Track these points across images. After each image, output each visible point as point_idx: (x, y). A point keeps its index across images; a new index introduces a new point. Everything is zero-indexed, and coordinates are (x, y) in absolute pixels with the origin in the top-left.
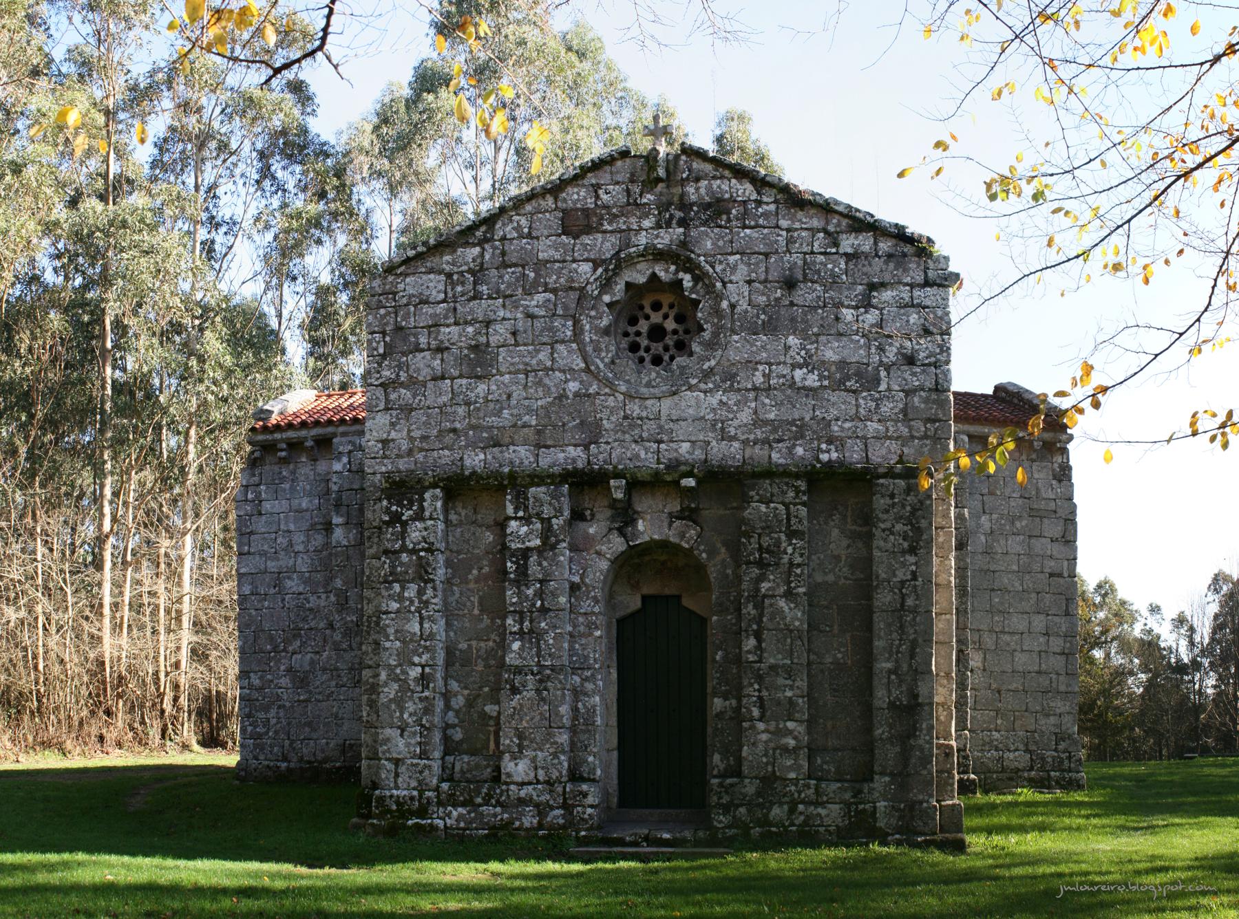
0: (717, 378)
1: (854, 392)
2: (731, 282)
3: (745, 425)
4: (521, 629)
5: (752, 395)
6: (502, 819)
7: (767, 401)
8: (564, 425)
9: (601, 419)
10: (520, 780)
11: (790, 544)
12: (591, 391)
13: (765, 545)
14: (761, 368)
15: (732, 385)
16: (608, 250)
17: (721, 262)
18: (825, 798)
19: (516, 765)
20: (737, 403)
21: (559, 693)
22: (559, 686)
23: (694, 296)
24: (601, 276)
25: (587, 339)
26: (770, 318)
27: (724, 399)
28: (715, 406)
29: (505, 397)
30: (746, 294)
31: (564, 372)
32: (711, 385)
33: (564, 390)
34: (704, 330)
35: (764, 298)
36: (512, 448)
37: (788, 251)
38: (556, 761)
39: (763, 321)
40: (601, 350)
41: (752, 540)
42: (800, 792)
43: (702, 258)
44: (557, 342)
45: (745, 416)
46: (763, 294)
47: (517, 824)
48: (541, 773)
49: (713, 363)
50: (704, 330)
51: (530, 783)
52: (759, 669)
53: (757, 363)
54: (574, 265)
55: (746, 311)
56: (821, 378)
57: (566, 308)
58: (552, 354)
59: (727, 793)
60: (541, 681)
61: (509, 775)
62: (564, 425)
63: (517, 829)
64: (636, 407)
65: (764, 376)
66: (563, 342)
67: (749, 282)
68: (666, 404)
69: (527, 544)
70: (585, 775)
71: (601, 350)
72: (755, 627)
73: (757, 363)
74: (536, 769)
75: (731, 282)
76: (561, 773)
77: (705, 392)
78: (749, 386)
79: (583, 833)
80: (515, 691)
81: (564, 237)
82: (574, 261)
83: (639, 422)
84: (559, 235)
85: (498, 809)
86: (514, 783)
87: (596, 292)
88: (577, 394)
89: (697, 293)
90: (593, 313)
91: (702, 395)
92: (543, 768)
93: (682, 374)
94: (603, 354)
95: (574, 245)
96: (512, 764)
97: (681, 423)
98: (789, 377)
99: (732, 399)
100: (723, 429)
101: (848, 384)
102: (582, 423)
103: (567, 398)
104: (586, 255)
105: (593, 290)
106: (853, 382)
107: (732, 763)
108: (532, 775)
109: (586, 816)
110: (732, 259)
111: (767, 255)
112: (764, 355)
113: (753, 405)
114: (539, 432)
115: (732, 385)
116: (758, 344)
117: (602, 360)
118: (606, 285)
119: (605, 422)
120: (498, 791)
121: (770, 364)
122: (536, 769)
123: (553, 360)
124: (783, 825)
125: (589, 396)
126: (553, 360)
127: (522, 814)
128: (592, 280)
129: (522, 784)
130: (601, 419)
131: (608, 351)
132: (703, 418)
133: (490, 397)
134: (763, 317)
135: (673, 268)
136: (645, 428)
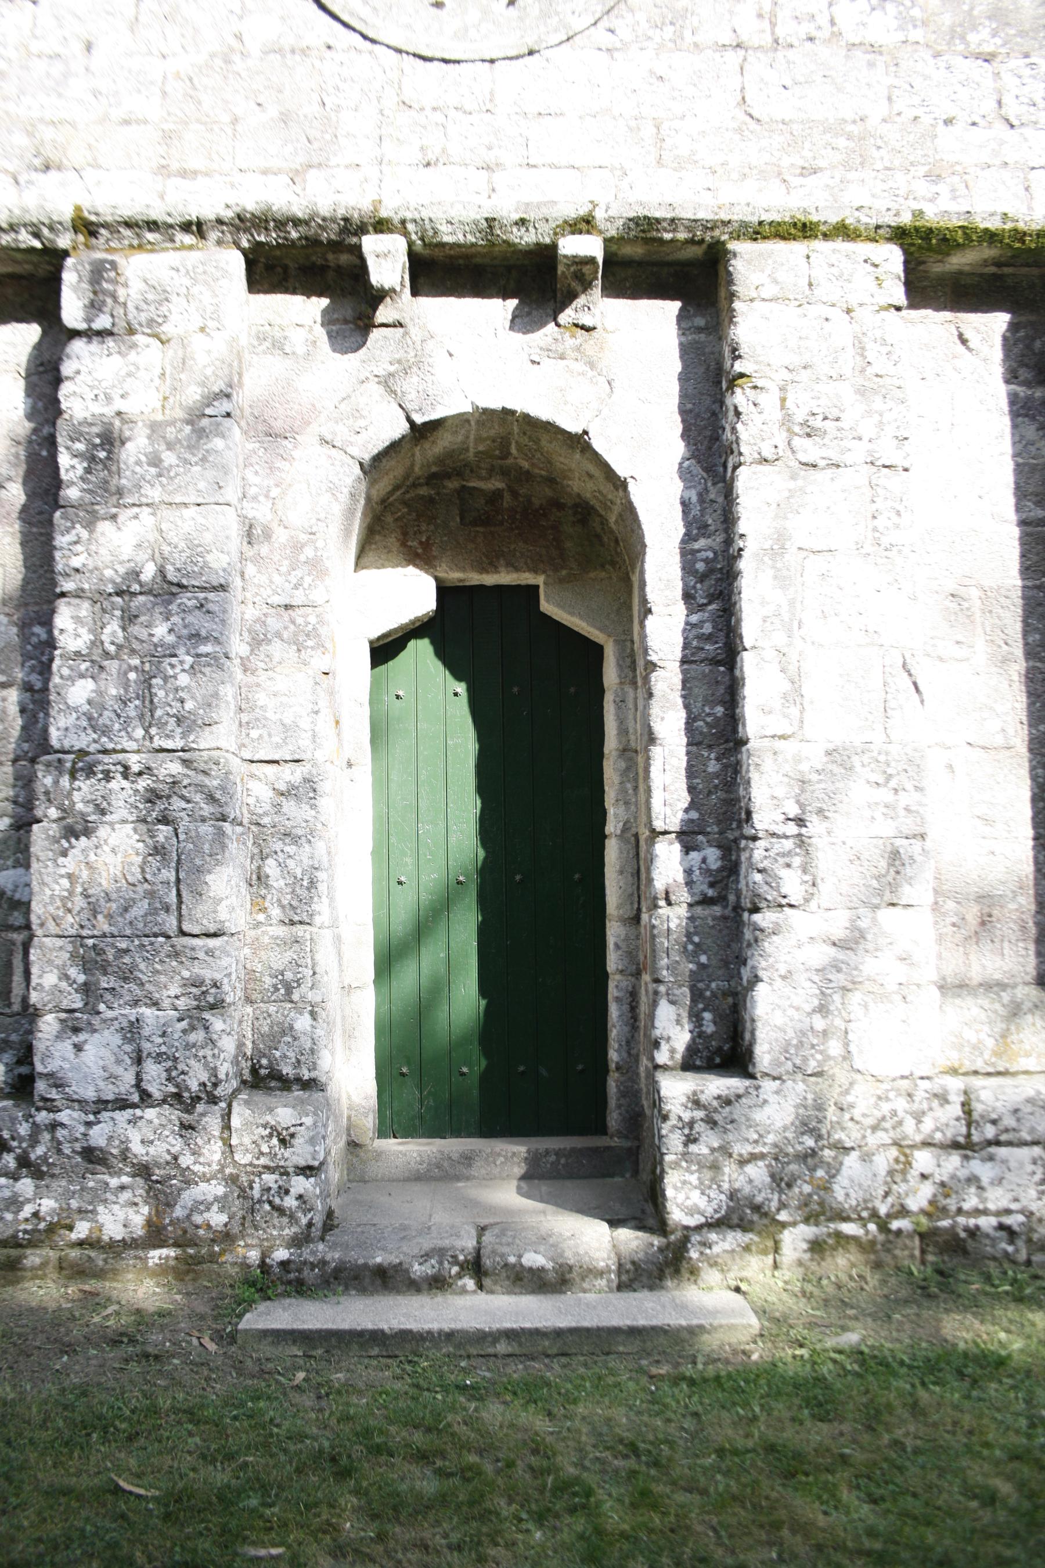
1: (988, 59)
4: (97, 642)
5: (734, 58)
6: (35, 1214)
8: (235, 121)
9: (338, 108)
10: (90, 1094)
11: (869, 413)
13: (800, 416)
18: (990, 1132)
19: (78, 1048)
21: (206, 829)
22: (207, 810)
29: (78, 47)
33: (239, 37)
36: (89, 173)
38: (198, 1036)
41: (761, 398)
42: (918, 1117)
47: (82, 1229)
48: (154, 1073)
51: (122, 1104)
52: (797, 760)
56: (906, 21)
59: (712, 1123)
60: (153, 797)
61: (57, 1082)
62: (235, 121)
63: (81, 1244)
69: (119, 405)
70: (287, 1070)
72: (780, 638)
74: (139, 1061)
76: (214, 1072)
79: (281, 1254)
80: (76, 829)
83: (438, 117)
85: (26, 1186)
86: (74, 1102)
92: (159, 1057)
96: (66, 1047)
98: (823, 20)
101: (973, 38)
102: (285, 119)
106: (985, 33)
107: (709, 1028)
108: (129, 1078)
109: (290, 1202)
114: (167, 137)
120: (24, 1129)
122: (139, 1061)
124: (874, 1215)
125: (305, 51)
127: (100, 1196)
129: (101, 1105)
130: (338, 108)
133: (35, 47)
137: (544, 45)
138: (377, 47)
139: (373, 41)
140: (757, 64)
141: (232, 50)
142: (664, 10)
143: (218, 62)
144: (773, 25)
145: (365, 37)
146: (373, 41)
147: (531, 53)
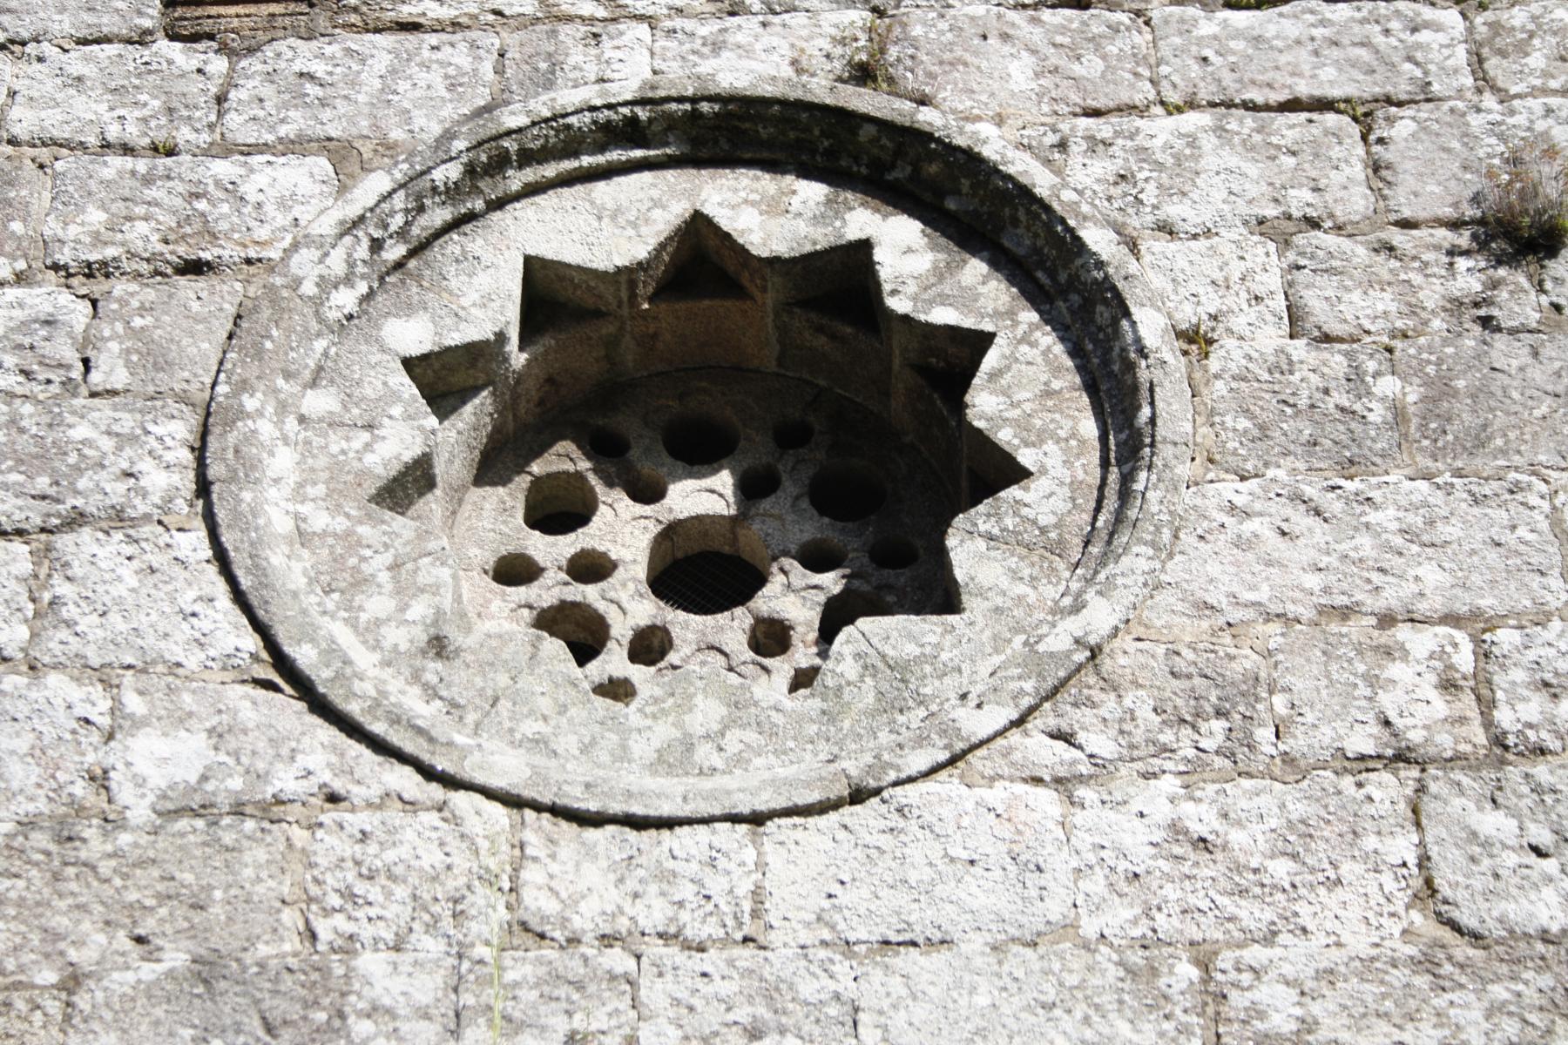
0: (1141, 702)
2: (1167, 229)
3: (1367, 966)
5: (1387, 789)
7: (1493, 823)
8: (73, 981)
9: (349, 946)
12: (285, 781)
14: (1420, 642)
15: (1238, 750)
16: (430, 102)
17: (1096, 145)
20: (1294, 840)
23: (942, 316)
24: (376, 212)
25: (281, 523)
26: (1440, 391)
27: (1200, 817)
28: (1142, 858)
30: (1272, 281)
31: (105, 677)
32: (1100, 743)
33: (100, 779)
34: (1019, 474)
35: (1385, 302)
37: (1484, 82)
39: (1398, 413)
40: (361, 582)
43: (986, 129)
44: (76, 520)
45: (1360, 913)
46: (1371, 283)
49: (1099, 617)
50: (1019, 474)
53: (1387, 620)
54: (223, 168)
55: (1283, 366)
57: (152, 356)
58: (34, 584)
62: (73, 981)
64: (594, 875)
65: (1448, 685)
66: (119, 518)
67: (1280, 230)
68: (801, 859)
71: (361, 582)
73: (1387, 620)
75: (1167, 229)
77: (1062, 783)
78: (1362, 741)
81: (164, 46)
82: (226, 149)
83: (618, 960)
84: (142, 39)
87: (345, 299)
88: (177, 808)
89: (966, 299)
90: (320, 402)
91: (1046, 801)
93: (889, 706)
94: (377, 605)
95: (230, 83)
97: (908, 960)
99: (1255, 814)
100: (1212, 996)
102: (207, 972)
103: (112, 823)
104: (296, 123)
105: (325, 269)
110: (1160, 130)
111: (1364, 115)
112: (1431, 575)
113: (1403, 847)
115: (1238, 750)
116: (1383, 517)
117: (369, 633)
118: (404, 256)
119: (371, 963)
121: (1478, 624)
123: (47, 612)
125: (272, 810)
126: (47, 612)
128: (326, 226)
130: (349, 946)
131: (405, 591)
132: (1069, 927)
134: (1388, 386)
135: (812, 192)
136: (654, 993)
137: (892, 776)
138: (460, 799)
139: (451, 782)
140: (1459, 805)
141: (80, 810)
142: (1197, 681)
143: (40, 839)
144: (1487, 705)
145: (428, 773)
146: (451, 782)
147: (858, 796)
